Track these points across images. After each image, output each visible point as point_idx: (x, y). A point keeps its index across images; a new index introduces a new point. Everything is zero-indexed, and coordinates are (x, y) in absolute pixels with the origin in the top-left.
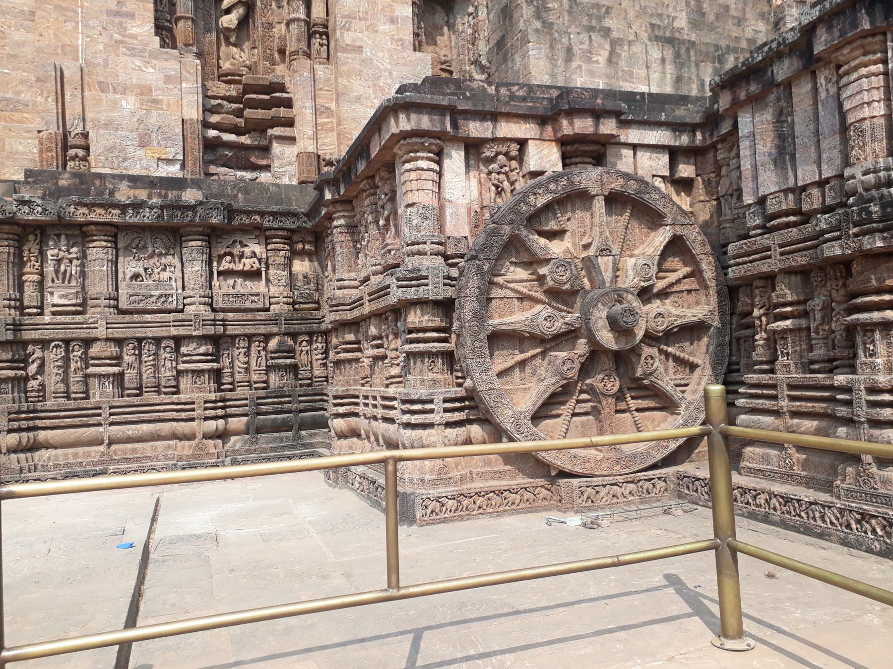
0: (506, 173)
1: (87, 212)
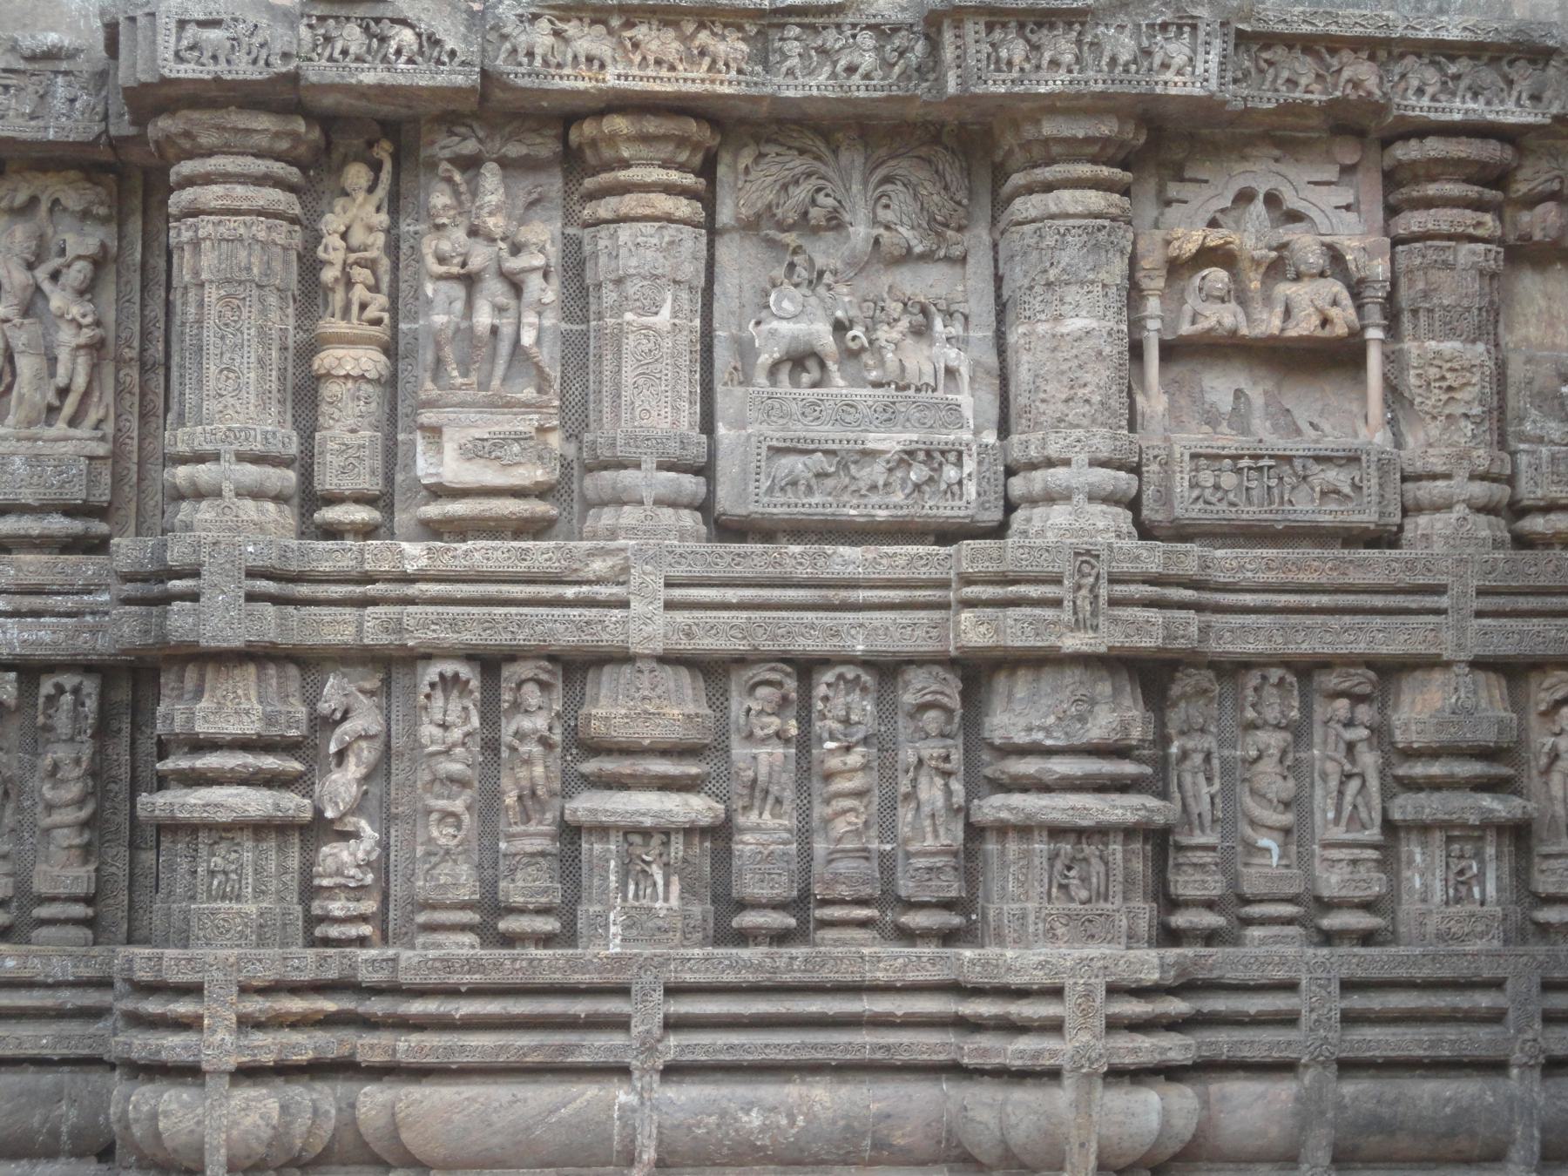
1: (604, 49)
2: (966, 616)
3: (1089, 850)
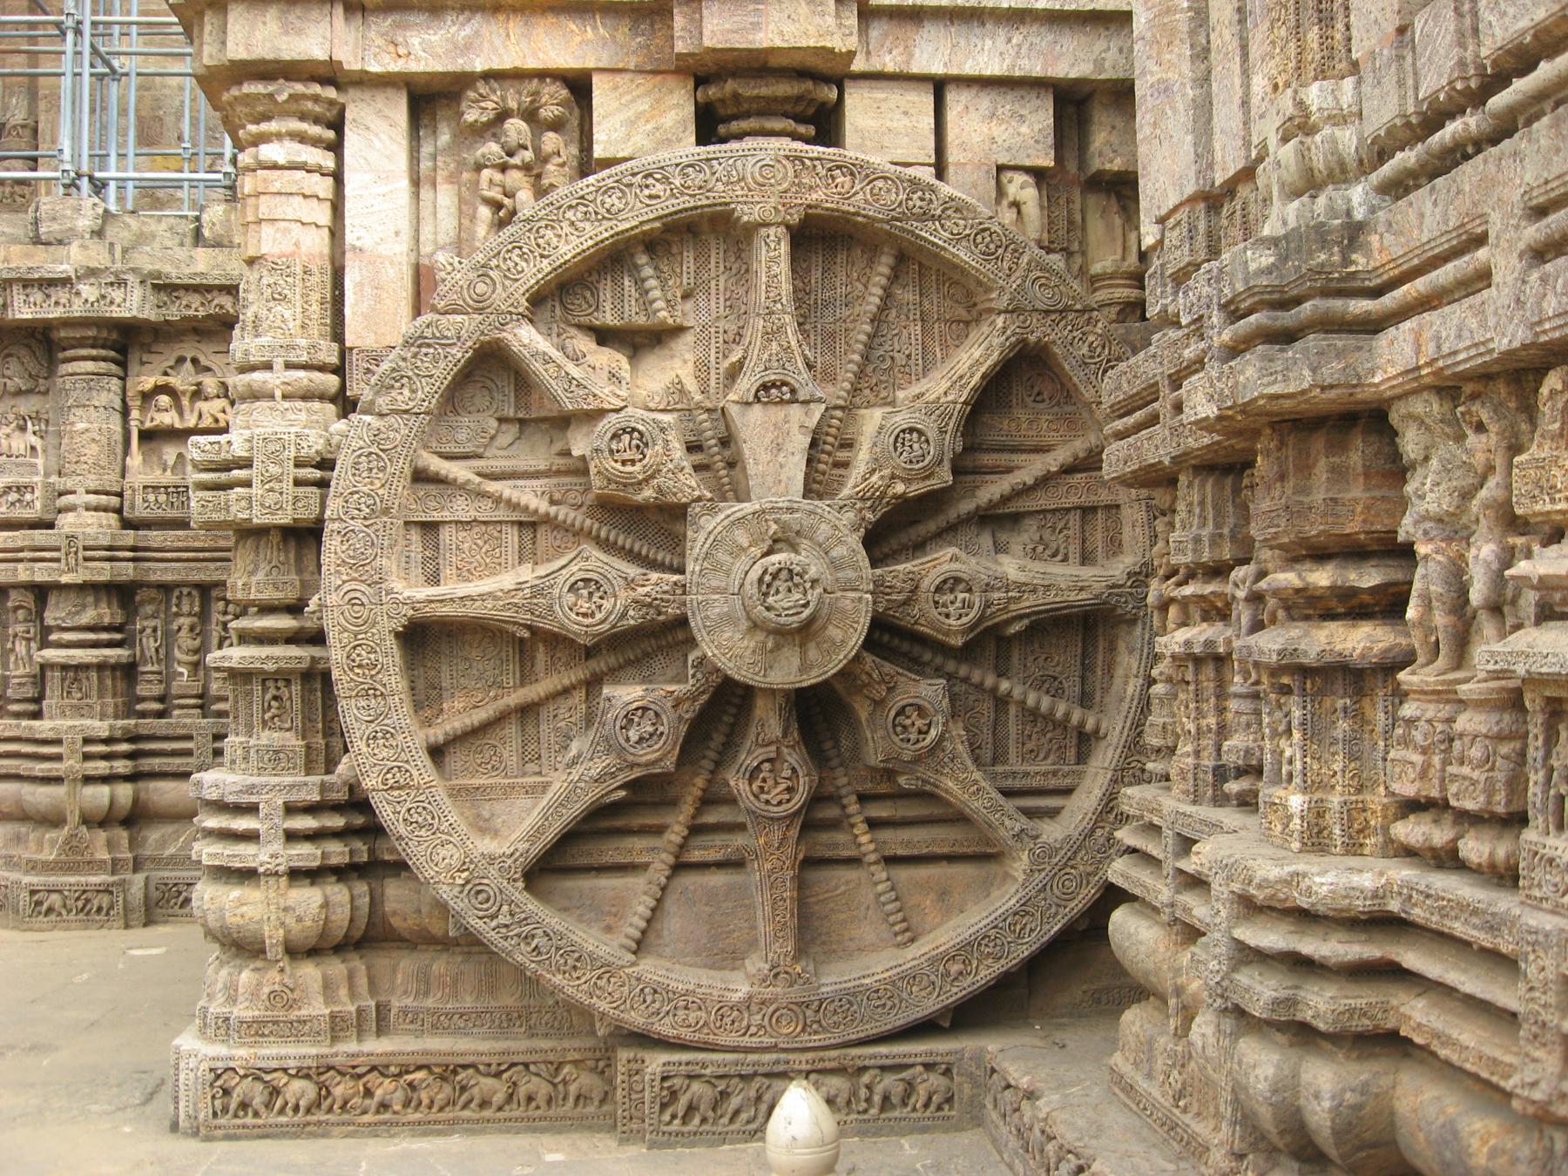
0: (526, 168)
2: (20, 566)
3: (82, 675)
